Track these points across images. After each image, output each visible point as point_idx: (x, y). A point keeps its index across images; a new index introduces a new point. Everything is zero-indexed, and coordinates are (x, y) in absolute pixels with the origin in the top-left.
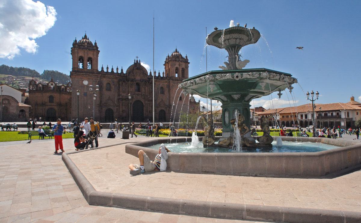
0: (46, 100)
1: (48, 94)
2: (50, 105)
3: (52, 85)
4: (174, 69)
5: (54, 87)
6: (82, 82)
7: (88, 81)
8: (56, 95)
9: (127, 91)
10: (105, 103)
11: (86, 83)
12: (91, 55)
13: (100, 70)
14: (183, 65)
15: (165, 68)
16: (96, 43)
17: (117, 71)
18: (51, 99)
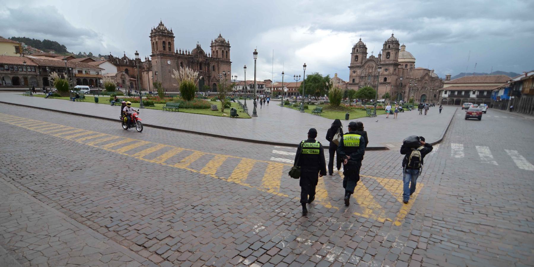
11: (169, 62)
12: (170, 41)
13: (175, 52)
15: (212, 50)
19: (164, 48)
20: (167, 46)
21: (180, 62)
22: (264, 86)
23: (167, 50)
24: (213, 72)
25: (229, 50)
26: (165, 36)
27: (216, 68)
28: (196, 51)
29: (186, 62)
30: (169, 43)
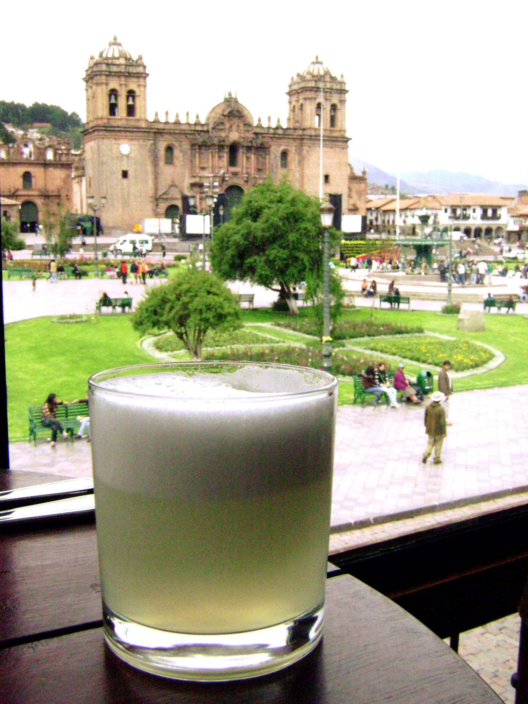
0: (19, 183)
1: (21, 170)
2: (24, 196)
3: (26, 146)
4: (314, 106)
5: (31, 153)
6: (119, 148)
7: (130, 145)
8: (37, 172)
9: (210, 165)
10: (164, 194)
12: (133, 86)
14: (335, 99)
15: (290, 103)
16: (140, 58)
17: (188, 118)
18: (27, 177)
19: (113, 109)
20: (122, 104)
21: (162, 146)
22: (502, 212)
23: (122, 111)
24: (281, 172)
25: (342, 102)
26: (119, 75)
27: (293, 158)
28: (219, 111)
29: (186, 146)
30: (131, 94)
